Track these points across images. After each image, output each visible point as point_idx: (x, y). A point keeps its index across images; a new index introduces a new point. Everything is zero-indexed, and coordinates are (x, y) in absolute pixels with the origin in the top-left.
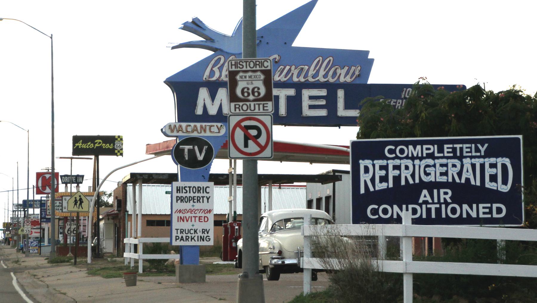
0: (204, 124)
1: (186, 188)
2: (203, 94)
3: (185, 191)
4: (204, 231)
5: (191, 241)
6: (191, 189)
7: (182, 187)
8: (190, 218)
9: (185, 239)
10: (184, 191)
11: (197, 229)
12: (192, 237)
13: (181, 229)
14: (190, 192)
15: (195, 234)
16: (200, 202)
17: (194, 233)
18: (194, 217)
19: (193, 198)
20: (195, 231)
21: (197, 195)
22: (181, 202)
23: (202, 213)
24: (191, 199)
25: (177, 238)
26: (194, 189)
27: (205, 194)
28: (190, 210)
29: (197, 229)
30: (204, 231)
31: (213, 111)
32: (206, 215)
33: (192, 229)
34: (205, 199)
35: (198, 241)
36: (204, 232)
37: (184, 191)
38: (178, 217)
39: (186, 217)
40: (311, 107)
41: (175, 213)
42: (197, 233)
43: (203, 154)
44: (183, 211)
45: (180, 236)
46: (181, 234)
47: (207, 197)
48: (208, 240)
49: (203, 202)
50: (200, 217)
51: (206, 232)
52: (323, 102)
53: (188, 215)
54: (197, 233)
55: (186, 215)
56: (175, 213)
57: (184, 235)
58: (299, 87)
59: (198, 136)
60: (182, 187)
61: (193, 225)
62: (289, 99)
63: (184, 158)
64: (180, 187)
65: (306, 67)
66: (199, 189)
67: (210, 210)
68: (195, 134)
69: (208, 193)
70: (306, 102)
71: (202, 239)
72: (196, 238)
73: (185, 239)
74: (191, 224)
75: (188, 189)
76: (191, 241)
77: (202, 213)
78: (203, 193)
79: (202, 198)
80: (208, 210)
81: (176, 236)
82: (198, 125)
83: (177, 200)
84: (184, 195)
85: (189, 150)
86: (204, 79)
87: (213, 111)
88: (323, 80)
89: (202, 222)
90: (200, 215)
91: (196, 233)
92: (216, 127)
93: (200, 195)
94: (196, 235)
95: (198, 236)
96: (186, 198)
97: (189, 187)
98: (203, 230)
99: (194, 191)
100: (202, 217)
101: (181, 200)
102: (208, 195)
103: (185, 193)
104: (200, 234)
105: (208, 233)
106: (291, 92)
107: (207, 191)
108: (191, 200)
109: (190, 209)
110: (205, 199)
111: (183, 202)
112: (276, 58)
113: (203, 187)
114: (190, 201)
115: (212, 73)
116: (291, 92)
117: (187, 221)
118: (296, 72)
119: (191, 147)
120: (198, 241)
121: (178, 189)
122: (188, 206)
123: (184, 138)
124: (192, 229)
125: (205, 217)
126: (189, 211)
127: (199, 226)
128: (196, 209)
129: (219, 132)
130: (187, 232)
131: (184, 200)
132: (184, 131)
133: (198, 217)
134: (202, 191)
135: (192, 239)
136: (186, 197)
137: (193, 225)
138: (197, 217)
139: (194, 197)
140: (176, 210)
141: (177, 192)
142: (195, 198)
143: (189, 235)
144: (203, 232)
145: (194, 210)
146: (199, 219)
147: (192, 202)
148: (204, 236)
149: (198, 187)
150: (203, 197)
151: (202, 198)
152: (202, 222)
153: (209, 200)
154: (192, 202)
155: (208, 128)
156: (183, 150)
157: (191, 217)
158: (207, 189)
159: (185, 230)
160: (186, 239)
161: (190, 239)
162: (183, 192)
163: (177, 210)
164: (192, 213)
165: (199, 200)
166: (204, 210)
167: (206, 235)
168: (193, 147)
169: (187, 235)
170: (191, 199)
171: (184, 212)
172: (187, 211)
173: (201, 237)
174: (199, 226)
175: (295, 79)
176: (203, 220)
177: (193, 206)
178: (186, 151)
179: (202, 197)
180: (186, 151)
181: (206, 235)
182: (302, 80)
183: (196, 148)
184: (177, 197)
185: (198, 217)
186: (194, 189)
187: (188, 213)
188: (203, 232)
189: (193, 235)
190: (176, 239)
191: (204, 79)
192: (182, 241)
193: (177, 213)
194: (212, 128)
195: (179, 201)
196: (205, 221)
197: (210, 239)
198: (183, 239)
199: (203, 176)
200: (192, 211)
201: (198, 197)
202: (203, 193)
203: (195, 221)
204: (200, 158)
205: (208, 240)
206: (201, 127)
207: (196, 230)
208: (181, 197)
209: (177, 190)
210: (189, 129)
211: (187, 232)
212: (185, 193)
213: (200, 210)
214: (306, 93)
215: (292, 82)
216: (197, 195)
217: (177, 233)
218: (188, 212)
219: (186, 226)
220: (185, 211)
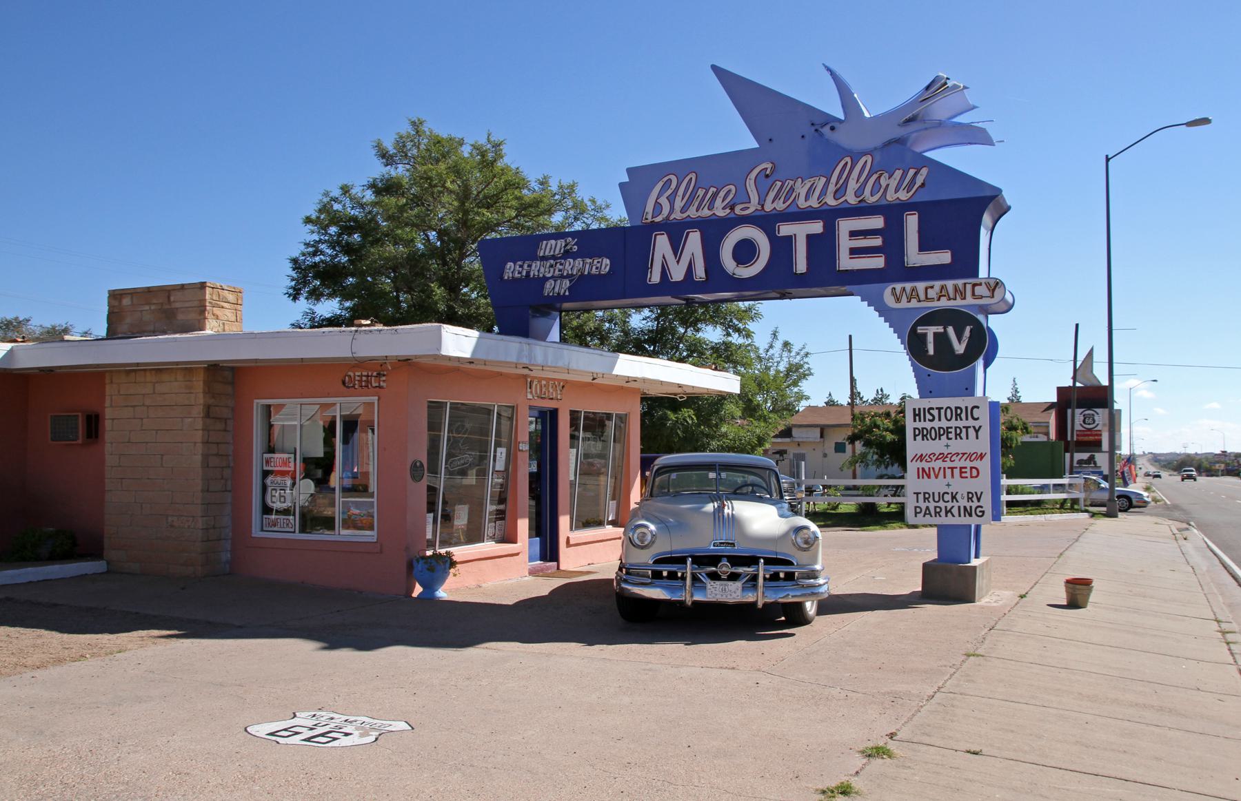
0: (960, 282)
1: (931, 411)
3: (931, 418)
5: (946, 516)
6: (943, 412)
7: (924, 409)
8: (942, 470)
9: (933, 514)
10: (928, 417)
12: (948, 509)
13: (925, 493)
14: (940, 420)
15: (952, 502)
16: (961, 438)
17: (950, 501)
18: (949, 468)
19: (947, 431)
20: (954, 497)
21: (953, 423)
22: (923, 439)
23: (965, 460)
24: (942, 433)
25: (918, 510)
26: (949, 411)
27: (971, 422)
28: (942, 456)
30: (970, 496)
33: (948, 493)
34: (971, 431)
35: (960, 516)
37: (928, 417)
38: (918, 469)
39: (933, 468)
41: (912, 461)
42: (957, 501)
44: (927, 457)
45: (923, 505)
46: (925, 502)
47: (974, 427)
48: (980, 514)
49: (967, 438)
50: (961, 468)
51: (975, 499)
53: (939, 464)
54: (957, 501)
55: (931, 465)
56: (912, 461)
57: (932, 505)
60: (924, 409)
61: (948, 485)
64: (919, 409)
66: (959, 411)
67: (982, 454)
68: (944, 303)
69: (978, 419)
72: (955, 511)
73: (933, 514)
74: (946, 481)
75: (935, 412)
76: (946, 516)
77: (965, 460)
78: (967, 419)
79: (964, 430)
80: (979, 455)
81: (916, 507)
82: (950, 284)
83: (915, 436)
84: (928, 425)
85: (935, 334)
89: (967, 477)
90: (962, 463)
91: (954, 500)
93: (960, 424)
95: (959, 507)
96: (933, 430)
97: (937, 408)
98: (968, 493)
99: (949, 417)
100: (966, 468)
101: (923, 436)
102: (977, 424)
103: (930, 420)
104: (963, 502)
105: (979, 500)
107: (975, 416)
108: (943, 434)
109: (940, 454)
110: (971, 431)
111: (928, 440)
113: (966, 408)
114: (940, 435)
117: (936, 477)
119: (940, 329)
120: (960, 516)
121: (917, 412)
122: (938, 446)
124: (948, 493)
125: (971, 468)
127: (962, 486)
128: (953, 453)
130: (937, 499)
131: (928, 436)
132: (922, 297)
134: (963, 415)
137: (948, 485)
138: (956, 468)
139: (948, 428)
141: (915, 421)
142: (950, 430)
143: (942, 504)
144: (970, 499)
145: (949, 456)
146: (961, 472)
148: (971, 507)
149: (956, 408)
150: (967, 428)
151: (964, 430)
152: (967, 477)
153: (979, 433)
155: (969, 287)
156: (925, 335)
157: (944, 468)
159: (933, 493)
160: (936, 512)
161: (943, 513)
162: (927, 420)
165: (959, 435)
168: (945, 328)
170: (942, 433)
171: (929, 460)
172: (936, 457)
173: (965, 508)
174: (962, 486)
176: (968, 475)
177: (947, 446)
178: (930, 338)
179: (964, 427)
180: (930, 338)
181: (974, 505)
183: (950, 330)
184: (915, 429)
185: (958, 469)
186: (949, 411)
188: (968, 498)
189: (949, 505)
190: (916, 513)
194: (977, 288)
195: (919, 438)
197: (983, 512)
200: (947, 457)
201: (956, 428)
202: (967, 419)
204: (960, 348)
205: (980, 514)
206: (956, 289)
208: (923, 429)
209: (915, 415)
210: (932, 293)
211: (937, 499)
212: (930, 420)
213: (961, 455)
216: (953, 423)
217: (917, 502)
218: (937, 459)
219: (935, 485)
220: (931, 456)
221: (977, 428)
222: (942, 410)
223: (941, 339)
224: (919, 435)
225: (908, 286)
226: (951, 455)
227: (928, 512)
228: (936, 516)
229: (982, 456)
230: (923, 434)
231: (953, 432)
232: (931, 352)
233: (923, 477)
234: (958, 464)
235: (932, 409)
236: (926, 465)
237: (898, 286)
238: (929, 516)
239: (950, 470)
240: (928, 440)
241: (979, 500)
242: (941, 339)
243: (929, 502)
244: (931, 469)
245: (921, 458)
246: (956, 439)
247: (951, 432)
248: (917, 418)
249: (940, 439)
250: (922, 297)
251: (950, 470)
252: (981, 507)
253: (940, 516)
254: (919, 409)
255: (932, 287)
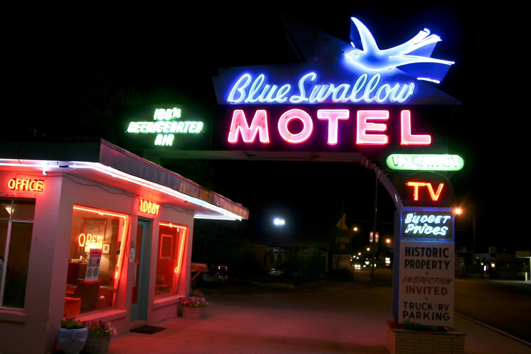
1: (417, 250)
5: (424, 318)
6: (425, 251)
7: (413, 248)
10: (415, 253)
11: (432, 304)
14: (423, 255)
21: (432, 258)
23: (439, 283)
26: (429, 251)
29: (432, 304)
37: (415, 253)
42: (432, 309)
49: (440, 268)
50: (436, 288)
61: (426, 299)
64: (409, 248)
75: (420, 251)
76: (424, 318)
91: (430, 308)
94: (430, 310)
103: (416, 256)
114: (422, 266)
135: (424, 316)
136: (418, 261)
137: (426, 299)
138: (432, 287)
139: (428, 261)
143: (421, 311)
145: (428, 279)
146: (435, 291)
147: (425, 267)
154: (425, 267)
161: (422, 316)
177: (427, 273)
186: (429, 251)
189: (427, 312)
201: (433, 261)
203: (429, 293)
213: (435, 280)
216: (432, 258)
246: (433, 268)
253: (420, 318)
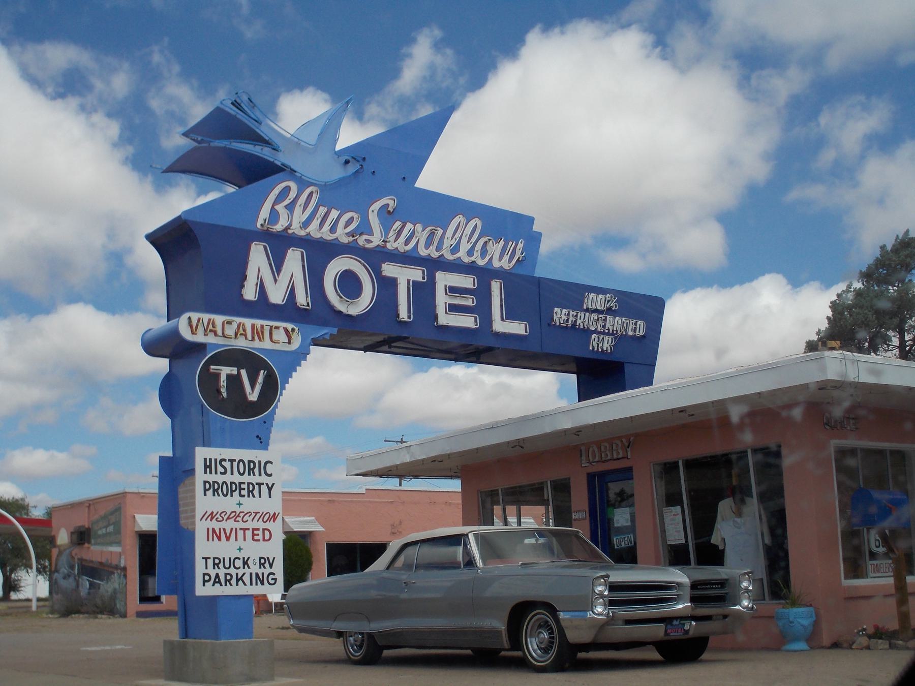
0: (259, 323)
1: (223, 463)
2: (258, 257)
3: (223, 471)
4: (264, 562)
5: (237, 585)
6: (235, 464)
7: (216, 460)
8: (234, 531)
10: (220, 469)
11: (249, 558)
12: (239, 577)
13: (214, 558)
14: (232, 474)
15: (244, 568)
16: (254, 496)
18: (241, 529)
20: (245, 563)
21: (246, 478)
22: (214, 495)
24: (234, 489)
25: (207, 578)
27: (264, 479)
29: (249, 558)
30: (263, 561)
31: (277, 296)
32: (267, 525)
33: (239, 559)
34: (264, 489)
35: (251, 584)
36: (263, 564)
37: (220, 469)
38: (208, 529)
39: (224, 529)
40: (453, 308)
41: (201, 520)
42: (249, 567)
43: (258, 388)
44: (218, 516)
46: (214, 568)
47: (267, 484)
48: (273, 582)
49: (260, 496)
50: (254, 530)
51: (267, 565)
52: (469, 302)
53: (229, 525)
54: (249, 567)
55: (223, 525)
56: (201, 520)
57: (222, 572)
58: (433, 265)
59: (250, 348)
60: (216, 460)
61: (240, 549)
62: (415, 287)
63: (219, 392)
64: (210, 460)
65: (440, 231)
67: (275, 514)
68: (241, 343)
69: (271, 475)
70: (442, 300)
71: (260, 580)
72: (246, 579)
75: (227, 465)
76: (237, 585)
78: (260, 475)
79: (257, 487)
81: (204, 575)
82: (248, 322)
83: (205, 490)
84: (220, 479)
85: (229, 377)
86: (259, 226)
87: (277, 296)
88: (466, 260)
89: (259, 540)
90: (255, 524)
91: (246, 566)
92: (282, 330)
94: (247, 570)
95: (251, 574)
97: (229, 460)
98: (260, 558)
99: (242, 471)
100: (258, 529)
101: (214, 491)
102: (269, 480)
103: (221, 473)
104: (255, 569)
105: (271, 566)
106: (417, 274)
107: (269, 472)
109: (232, 512)
110: (264, 489)
111: (219, 495)
112: (388, 205)
113: (260, 462)
114: (232, 491)
115: (274, 216)
116: (417, 274)
117: (228, 539)
118: (425, 234)
119: (234, 370)
120: (251, 584)
121: (208, 464)
122: (228, 504)
123: (221, 348)
124: (239, 559)
125: (264, 530)
126: (231, 516)
128: (245, 513)
129: (289, 343)
130: (227, 565)
131: (220, 491)
132: (220, 333)
133: (251, 530)
134: (256, 470)
135: (238, 580)
137: (240, 549)
138: (248, 529)
139: (240, 483)
140: (205, 512)
141: (205, 472)
142: (242, 486)
143: (232, 571)
144: (262, 565)
145: (242, 515)
146: (254, 535)
147: (236, 494)
148: (263, 574)
149: (249, 462)
150: (260, 484)
151: (257, 487)
152: (259, 540)
154: (236, 494)
156: (217, 376)
157: (236, 529)
158: (268, 465)
159: (224, 558)
160: (226, 580)
161: (234, 581)
162: (218, 472)
163: (206, 512)
164: (238, 521)
165: (252, 491)
166: (263, 513)
167: (267, 570)
169: (227, 571)
170: (234, 489)
171: (220, 519)
173: (257, 574)
174: (254, 550)
175: (423, 252)
176: (260, 537)
177: (240, 504)
178: (223, 378)
179: (257, 484)
180: (223, 378)
181: (267, 570)
182: (435, 255)
183: (243, 372)
184: (205, 482)
187: (228, 520)
188: (261, 564)
190: (205, 582)
191: (259, 226)
192: (216, 584)
193: (206, 520)
195: (210, 493)
196: (264, 540)
197: (275, 580)
198: (219, 580)
199: (258, 437)
200: (239, 516)
201: (249, 484)
202: (260, 475)
203: (245, 540)
204: (253, 396)
205: (273, 582)
207: (245, 560)
208: (214, 482)
209: (206, 467)
210: (230, 331)
211: (227, 565)
212: (221, 473)
214: (444, 279)
215: (416, 255)
216: (246, 478)
217: (206, 568)
218: (228, 518)
219: (225, 550)
220: (223, 515)
221: (270, 486)
222: (234, 463)
223: (234, 381)
224: (209, 489)
225: (206, 317)
226: (244, 514)
227: (217, 580)
228: (226, 585)
229: (274, 517)
230: (213, 488)
231: (246, 489)
232: (225, 395)
233: (213, 540)
234: (251, 525)
235: (225, 460)
236: (216, 525)
237: (195, 316)
238: (219, 584)
239: (242, 531)
240: (219, 495)
241: (271, 566)
242: (234, 381)
243: (219, 568)
244: (222, 531)
245: (212, 516)
246: (249, 496)
247: (244, 489)
248: (208, 470)
249: (232, 496)
250: (220, 333)
251: (242, 531)
252: (274, 574)
254: (210, 460)
255: (229, 323)
